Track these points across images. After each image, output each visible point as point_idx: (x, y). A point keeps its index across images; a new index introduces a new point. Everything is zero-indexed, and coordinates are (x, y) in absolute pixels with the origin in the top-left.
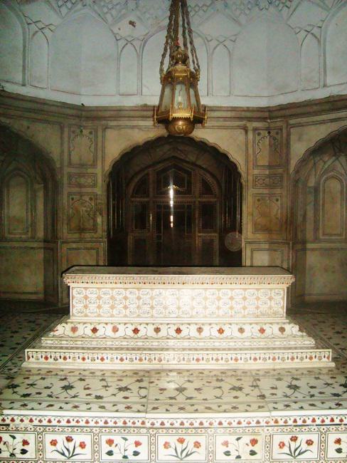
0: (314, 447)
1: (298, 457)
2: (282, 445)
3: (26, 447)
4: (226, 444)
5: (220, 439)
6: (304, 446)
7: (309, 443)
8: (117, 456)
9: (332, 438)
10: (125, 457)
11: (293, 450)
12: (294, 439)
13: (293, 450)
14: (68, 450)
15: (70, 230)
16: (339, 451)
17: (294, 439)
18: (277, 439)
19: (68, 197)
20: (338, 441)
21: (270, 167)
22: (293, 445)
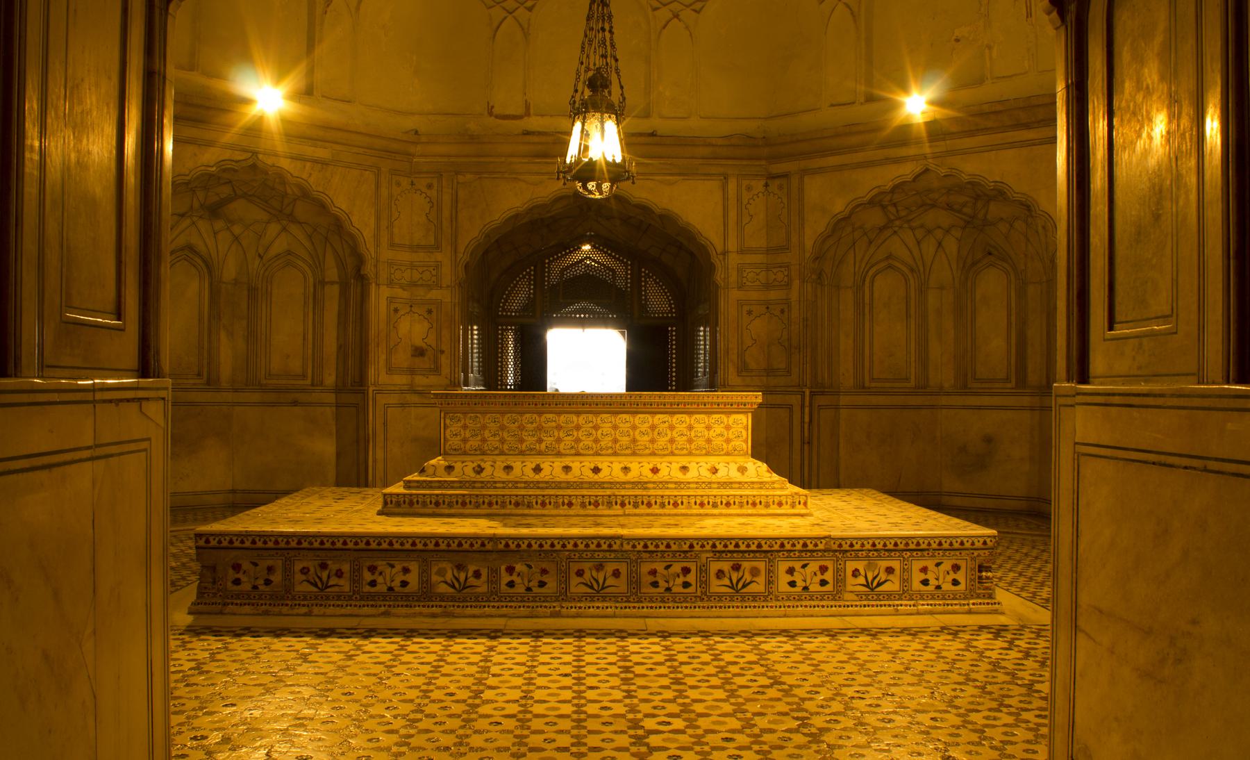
0: (761, 579)
1: (744, 590)
2: (720, 574)
3: (407, 578)
4: (653, 572)
5: (646, 568)
6: (748, 577)
7: (755, 572)
8: (520, 589)
9: (783, 566)
10: (529, 589)
11: (735, 582)
12: (736, 568)
13: (735, 582)
14: (458, 580)
15: (390, 370)
16: (793, 584)
17: (736, 568)
18: (715, 567)
19: (388, 307)
20: (791, 571)
21: (769, 251)
22: (735, 577)
